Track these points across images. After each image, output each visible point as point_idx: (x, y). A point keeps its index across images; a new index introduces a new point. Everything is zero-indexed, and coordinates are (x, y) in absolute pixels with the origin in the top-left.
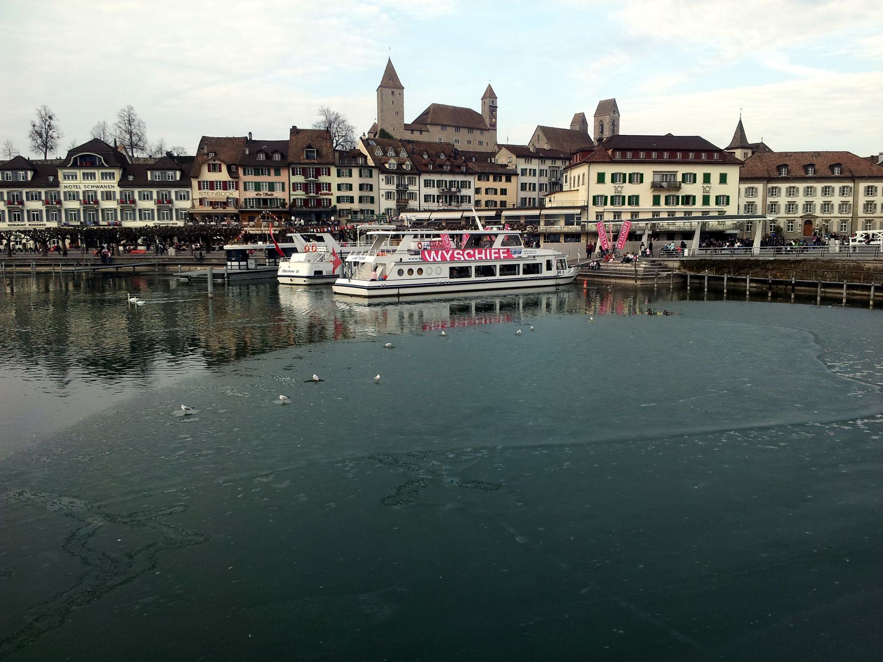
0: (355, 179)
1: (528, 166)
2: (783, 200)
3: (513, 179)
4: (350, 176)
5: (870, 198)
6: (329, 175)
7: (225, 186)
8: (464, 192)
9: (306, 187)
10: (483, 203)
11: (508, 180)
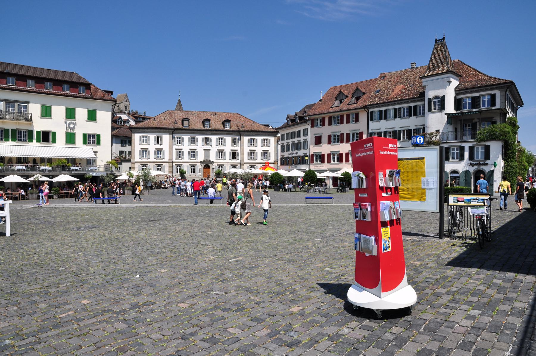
2: (186, 147)
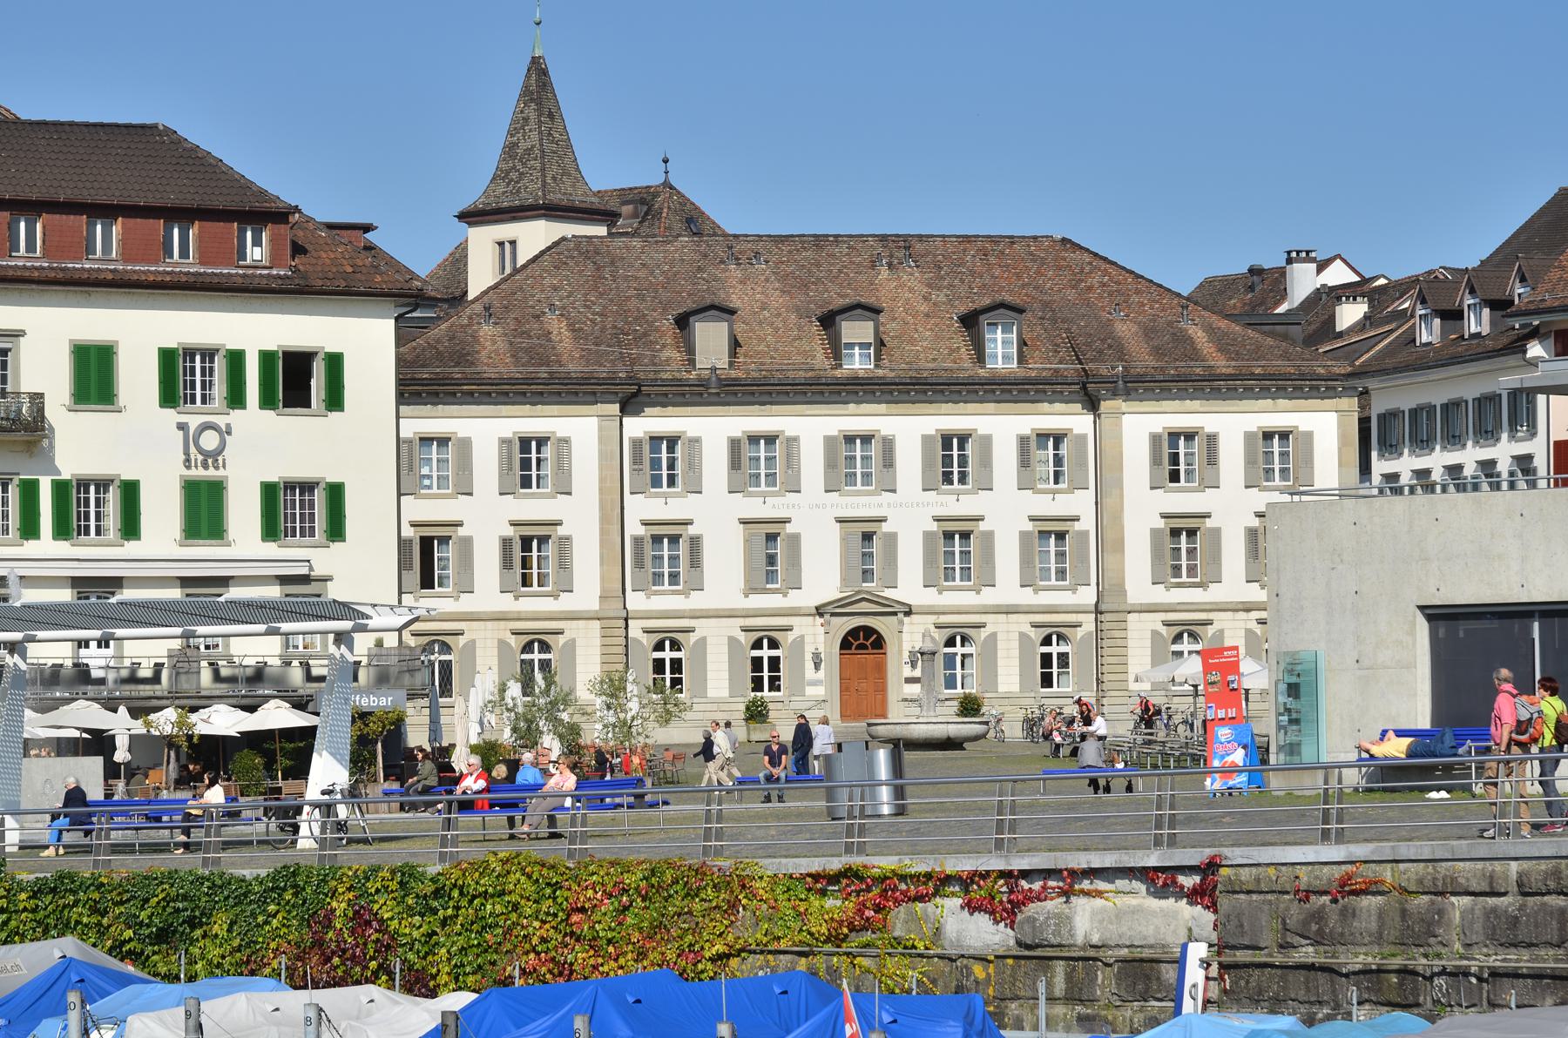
5: (1182, 501)
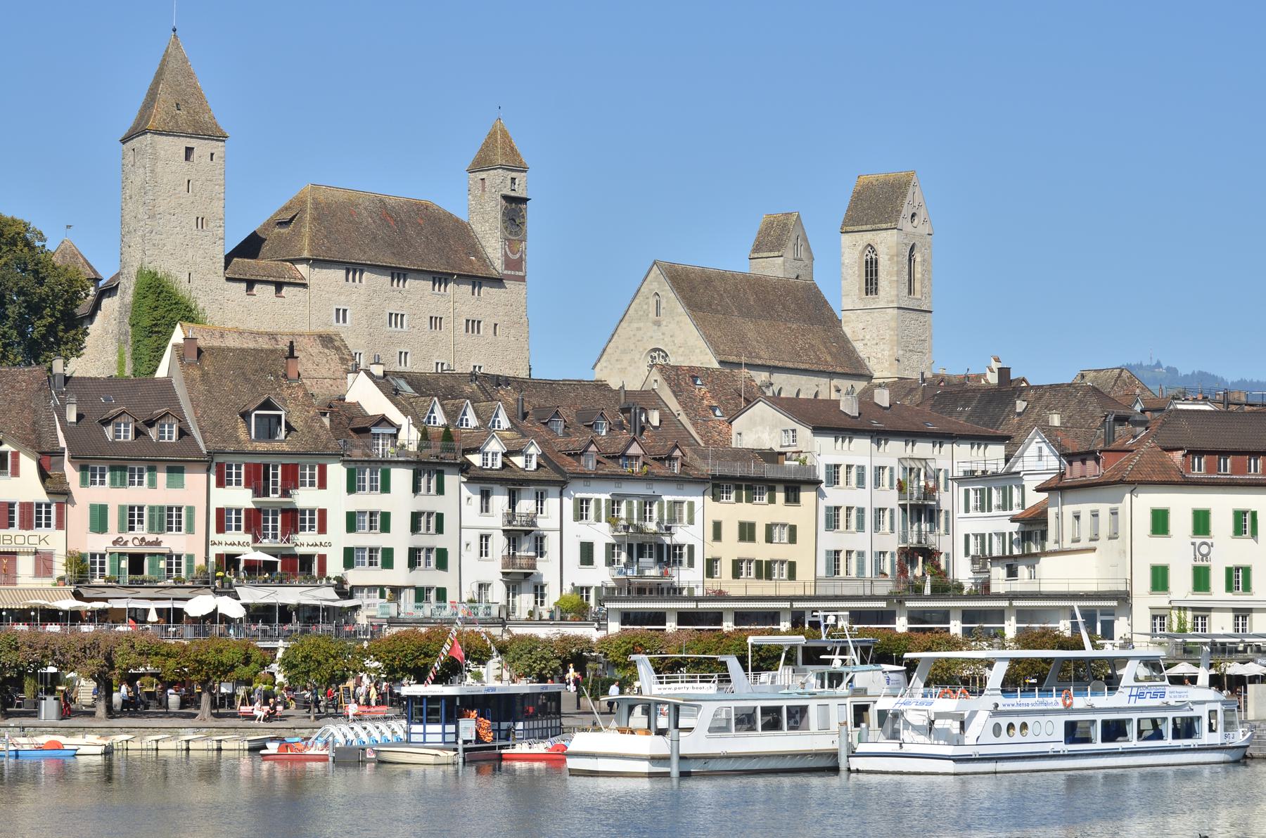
0: (400, 497)
1: (843, 460)
3: (807, 496)
4: (386, 488)
6: (323, 485)
7: (32, 516)
8: (682, 535)
9: (254, 521)
10: (725, 569)
11: (793, 499)
